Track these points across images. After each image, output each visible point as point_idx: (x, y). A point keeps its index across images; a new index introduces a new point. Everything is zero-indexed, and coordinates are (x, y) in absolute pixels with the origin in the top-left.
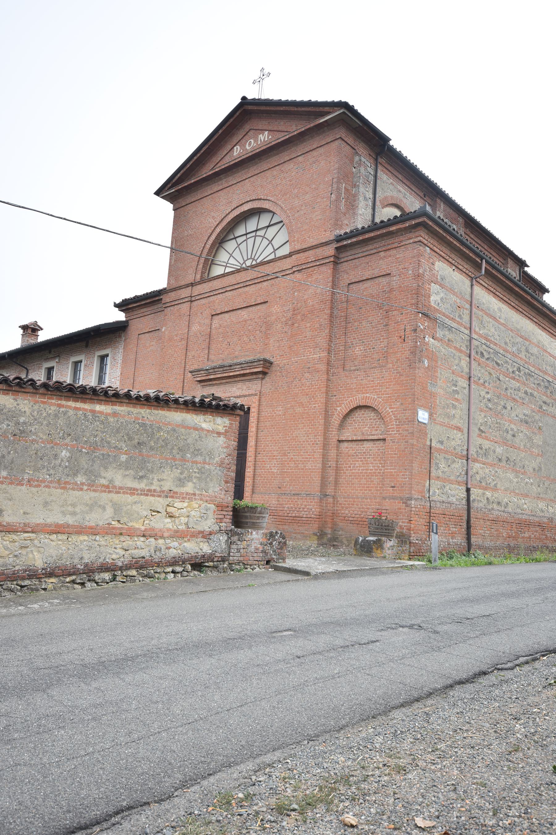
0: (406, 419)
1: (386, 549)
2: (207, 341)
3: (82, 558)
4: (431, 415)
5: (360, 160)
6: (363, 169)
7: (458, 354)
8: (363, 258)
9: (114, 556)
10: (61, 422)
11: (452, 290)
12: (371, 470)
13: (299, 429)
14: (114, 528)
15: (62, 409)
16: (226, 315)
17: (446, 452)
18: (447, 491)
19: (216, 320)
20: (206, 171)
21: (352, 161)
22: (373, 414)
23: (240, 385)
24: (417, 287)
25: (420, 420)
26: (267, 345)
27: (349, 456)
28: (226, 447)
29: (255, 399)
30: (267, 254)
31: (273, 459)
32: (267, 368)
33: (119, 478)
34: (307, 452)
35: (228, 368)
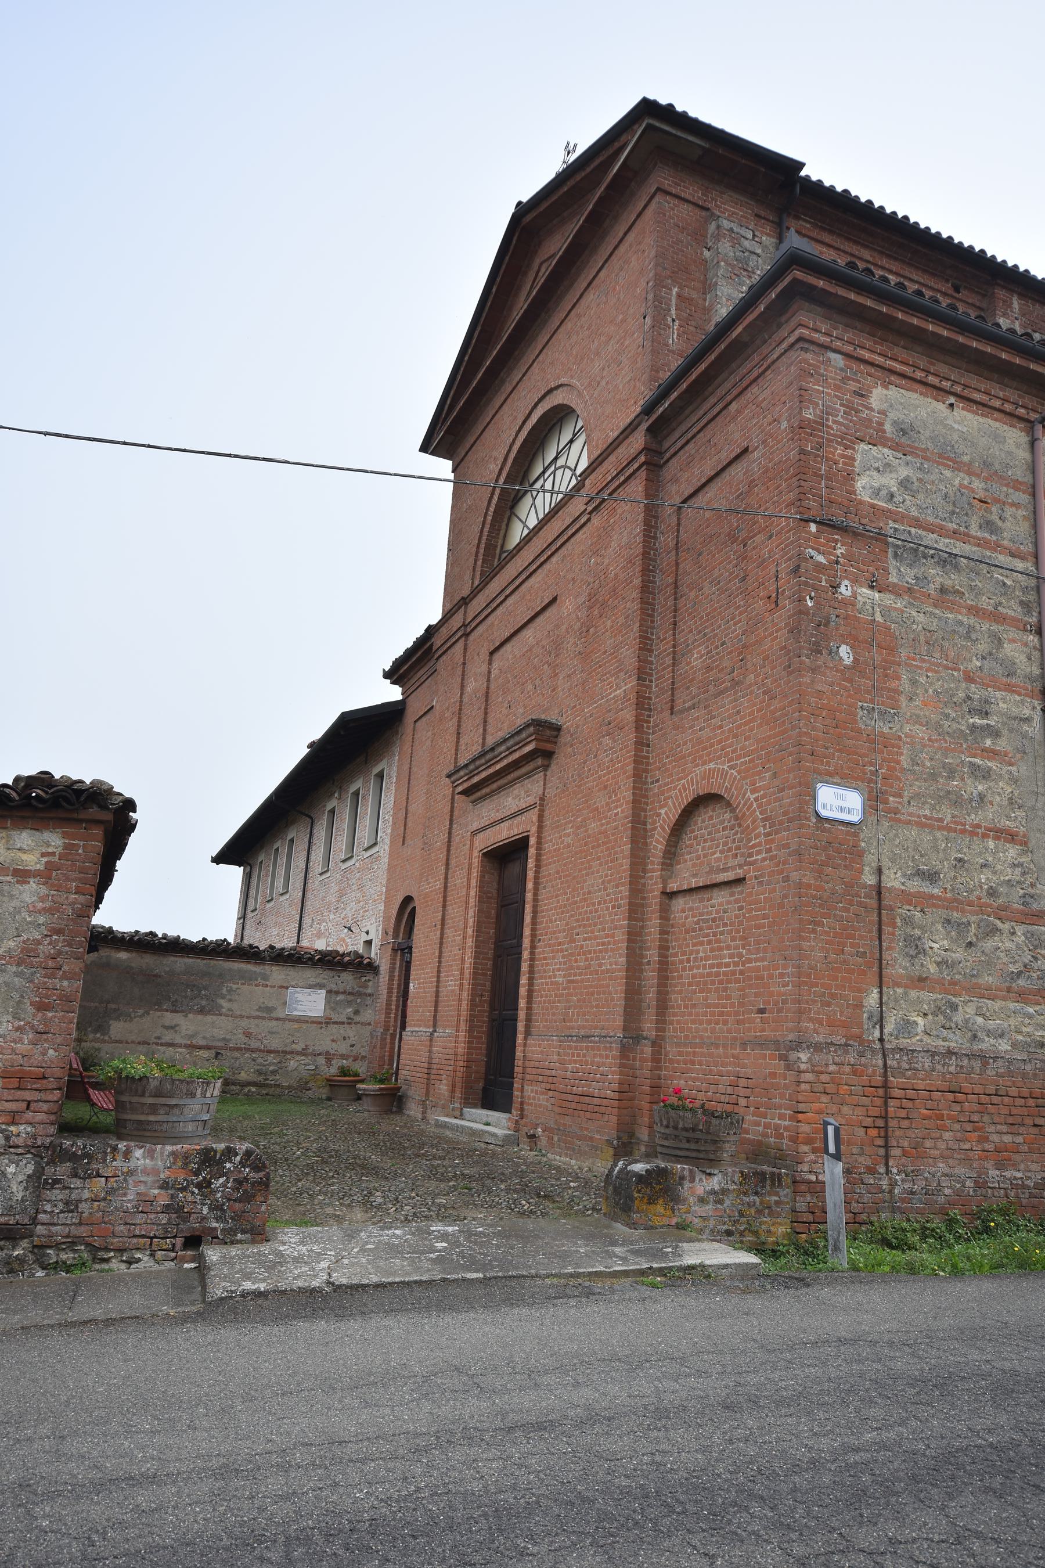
0: (785, 814)
1: (691, 1200)
4: (873, 802)
5: (718, 227)
6: (728, 244)
7: (985, 626)
8: (701, 434)
11: (948, 458)
12: (727, 965)
16: (508, 647)
17: (955, 903)
18: (966, 1021)
22: (727, 816)
23: (517, 790)
24: (797, 457)
25: (824, 813)
26: (554, 690)
28: (45, 911)
29: (533, 815)
31: (558, 951)
32: (548, 741)
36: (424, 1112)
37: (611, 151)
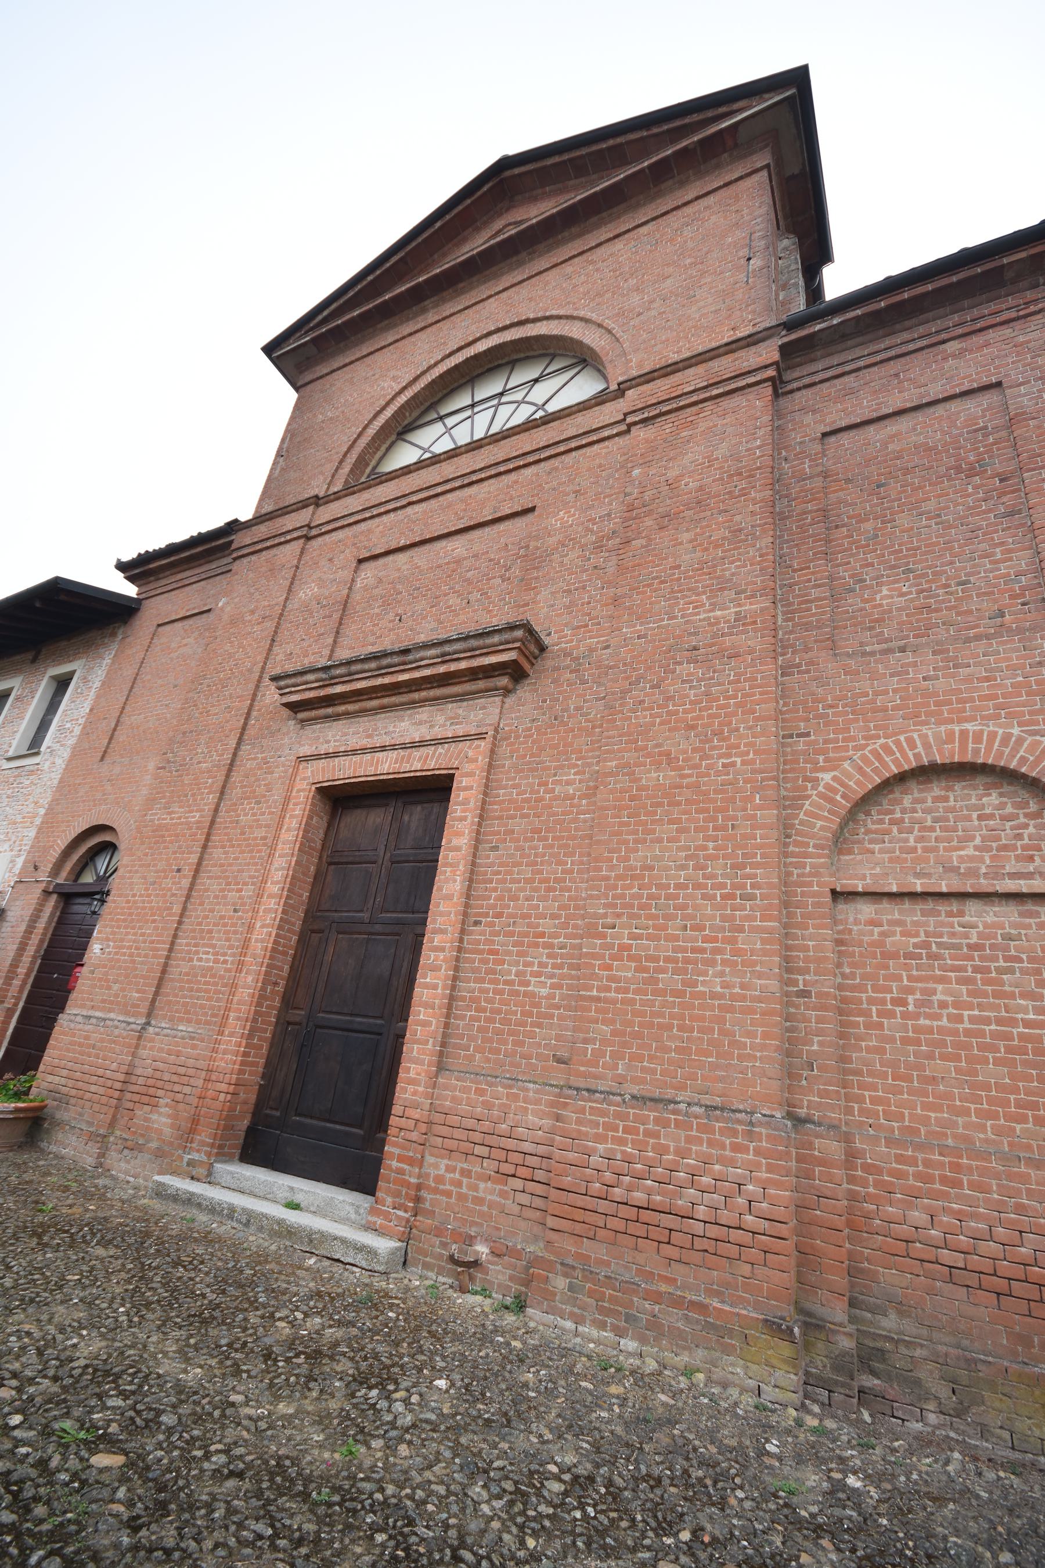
2: (336, 616)
13: (660, 840)
16: (401, 558)
22: (993, 799)
23: (424, 713)
27: (886, 955)
31: (536, 945)
34: (700, 928)
35: (396, 659)
36: (102, 1155)
37: (710, 114)
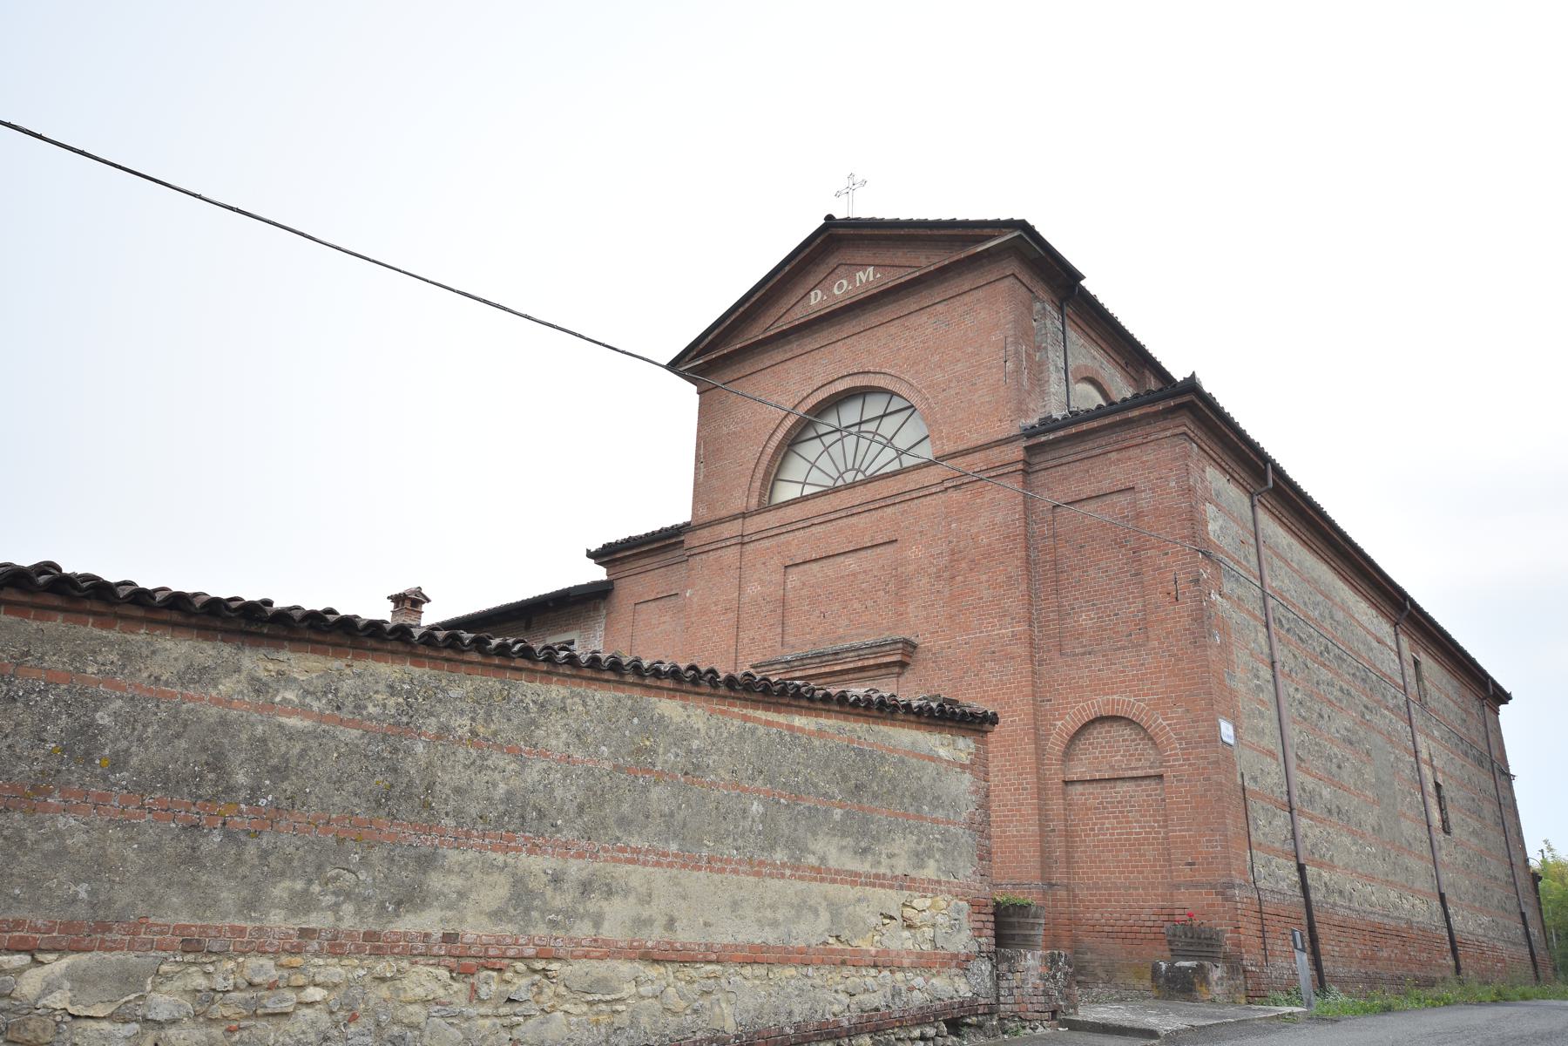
2: (779, 611)
3: (790, 1013)
4: (1236, 730)
9: (836, 1008)
10: (748, 748)
14: (833, 951)
15: (749, 725)
16: (814, 566)
19: (794, 577)
20: (756, 333)
21: (1030, 309)
22: (1128, 732)
30: (885, 460)
33: (830, 850)
